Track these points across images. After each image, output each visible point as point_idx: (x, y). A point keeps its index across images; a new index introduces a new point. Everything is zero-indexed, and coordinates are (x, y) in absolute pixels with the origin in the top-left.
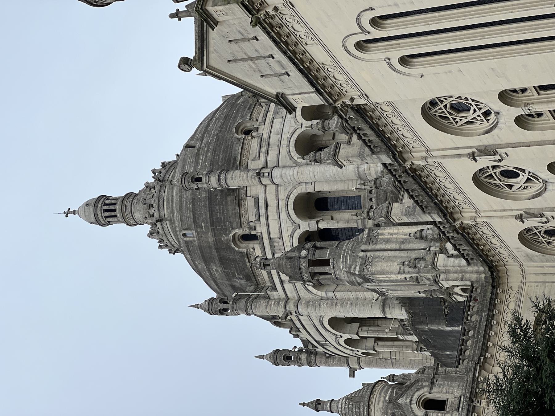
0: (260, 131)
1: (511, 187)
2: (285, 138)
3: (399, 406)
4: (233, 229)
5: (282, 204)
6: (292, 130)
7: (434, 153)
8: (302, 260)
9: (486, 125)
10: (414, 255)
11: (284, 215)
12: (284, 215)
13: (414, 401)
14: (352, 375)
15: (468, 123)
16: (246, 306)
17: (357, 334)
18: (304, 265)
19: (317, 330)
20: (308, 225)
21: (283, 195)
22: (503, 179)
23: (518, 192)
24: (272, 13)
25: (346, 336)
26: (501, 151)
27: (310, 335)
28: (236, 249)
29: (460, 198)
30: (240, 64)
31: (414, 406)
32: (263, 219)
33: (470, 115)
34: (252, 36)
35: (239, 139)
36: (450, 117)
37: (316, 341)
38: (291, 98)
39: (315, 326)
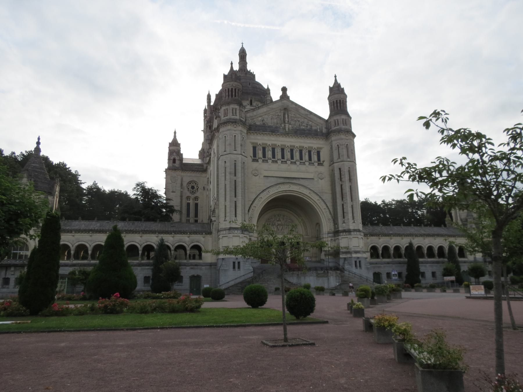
14: (202, 131)
31: (173, 157)
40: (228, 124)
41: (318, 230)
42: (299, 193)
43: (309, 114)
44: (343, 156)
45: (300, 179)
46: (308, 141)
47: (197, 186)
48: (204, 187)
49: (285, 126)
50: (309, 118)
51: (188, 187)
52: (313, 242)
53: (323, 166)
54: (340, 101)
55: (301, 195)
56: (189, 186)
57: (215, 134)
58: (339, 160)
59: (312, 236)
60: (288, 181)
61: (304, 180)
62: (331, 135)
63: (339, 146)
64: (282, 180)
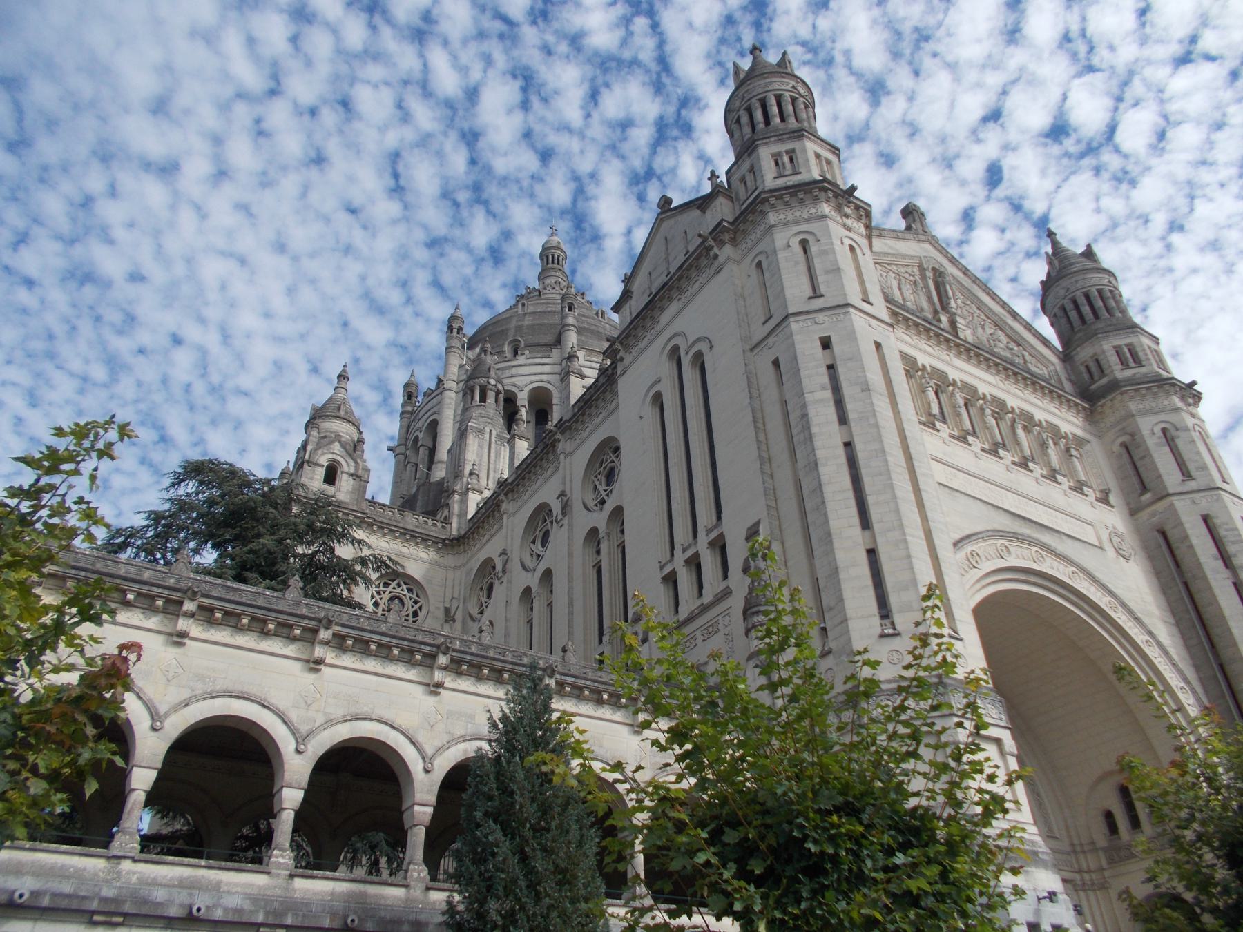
1: (534, 542)
3: (331, 442)
9: (591, 504)
10: (483, 475)
11: (533, 378)
12: (533, 378)
13: (335, 457)
18: (482, 381)
20: (523, 398)
22: (542, 533)
23: (528, 549)
24: (712, 254)
29: (525, 497)
41: (1109, 816)
42: (1074, 599)
44: (1204, 468)
45: (1064, 537)
47: (416, 602)
48: (447, 610)
49: (953, 323)
50: (1011, 328)
51: (378, 597)
52: (1087, 877)
56: (378, 593)
57: (716, 250)
58: (1192, 485)
59: (1072, 845)
61: (1077, 544)
62: (1126, 392)
63: (1174, 433)
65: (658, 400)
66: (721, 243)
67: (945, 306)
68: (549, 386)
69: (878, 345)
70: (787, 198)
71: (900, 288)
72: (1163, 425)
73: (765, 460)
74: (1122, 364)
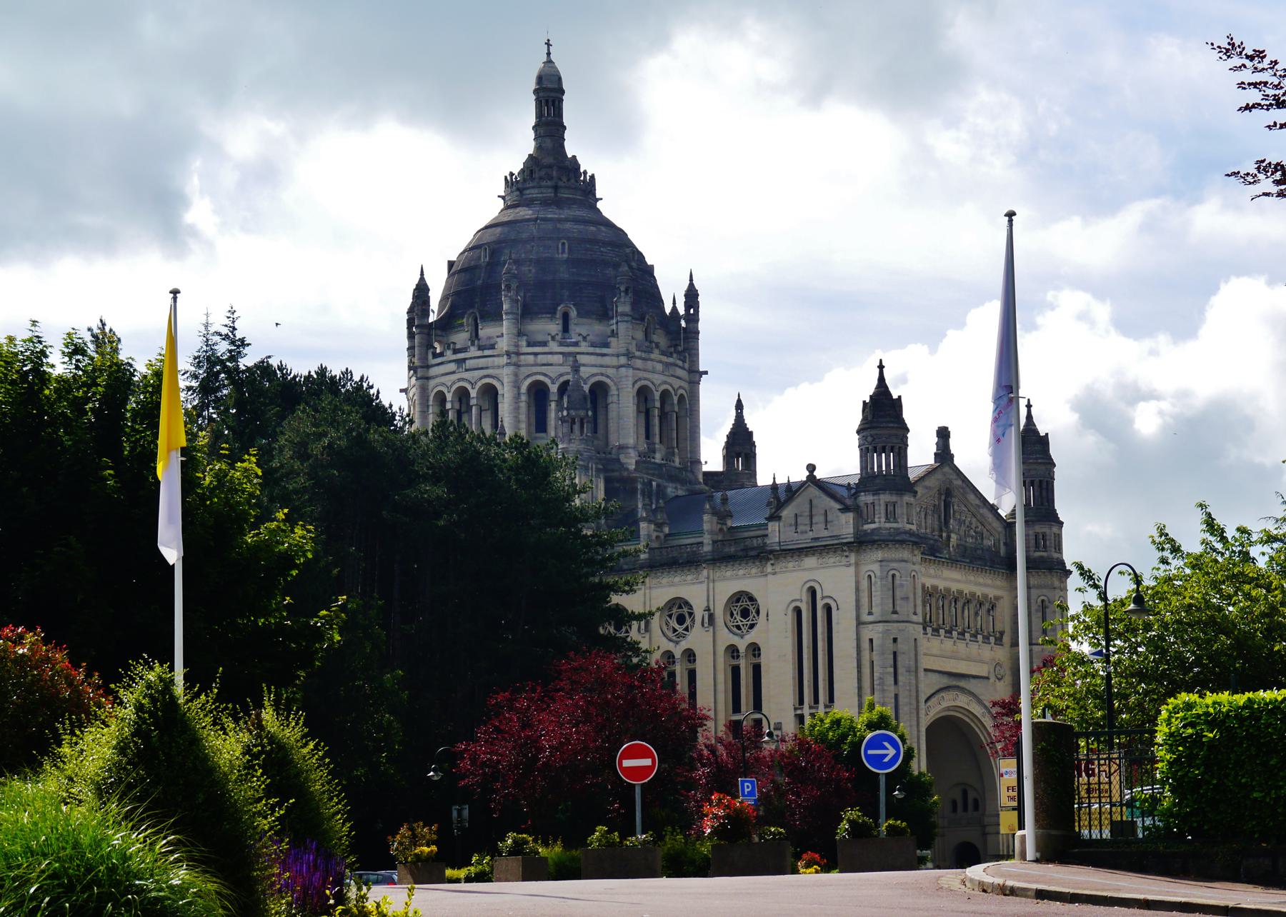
0: (656, 351)
1: (670, 616)
2: (650, 376)
4: (574, 305)
5: (603, 370)
6: (655, 381)
7: (711, 585)
8: (585, 411)
9: (730, 624)
11: (595, 370)
12: (595, 370)
15: (732, 615)
16: (514, 314)
17: (477, 405)
18: (582, 413)
19: (482, 368)
21: (610, 372)
24: (846, 554)
25: (473, 393)
26: (711, 629)
27: (475, 358)
28: (559, 308)
29: (665, 581)
30: (808, 506)
32: (591, 350)
33: (739, 618)
34: (828, 527)
35: (642, 319)
36: (739, 604)
37: (464, 360)
38: (777, 524)
39: (487, 368)
40: (904, 546)
42: (966, 713)
43: (981, 504)
46: (981, 580)
49: (949, 537)
50: (981, 515)
53: (1002, 645)
54: (1041, 481)
55: (969, 717)
60: (954, 683)
63: (1047, 602)
64: (945, 681)
65: (798, 612)
66: (851, 551)
67: (947, 522)
68: (608, 381)
69: (915, 639)
70: (890, 546)
71: (925, 518)
72: (1042, 598)
73: (860, 688)
74: (1036, 547)
